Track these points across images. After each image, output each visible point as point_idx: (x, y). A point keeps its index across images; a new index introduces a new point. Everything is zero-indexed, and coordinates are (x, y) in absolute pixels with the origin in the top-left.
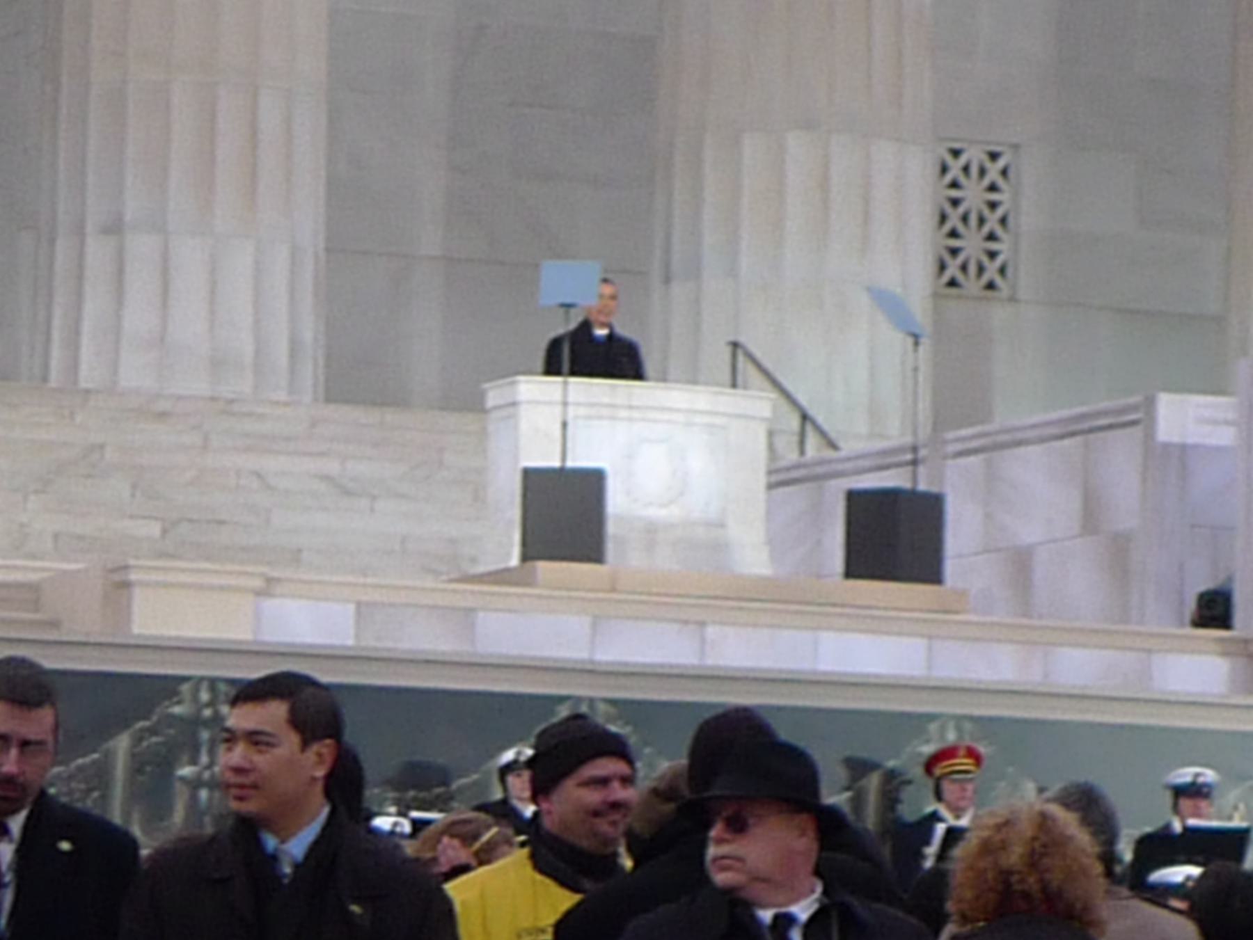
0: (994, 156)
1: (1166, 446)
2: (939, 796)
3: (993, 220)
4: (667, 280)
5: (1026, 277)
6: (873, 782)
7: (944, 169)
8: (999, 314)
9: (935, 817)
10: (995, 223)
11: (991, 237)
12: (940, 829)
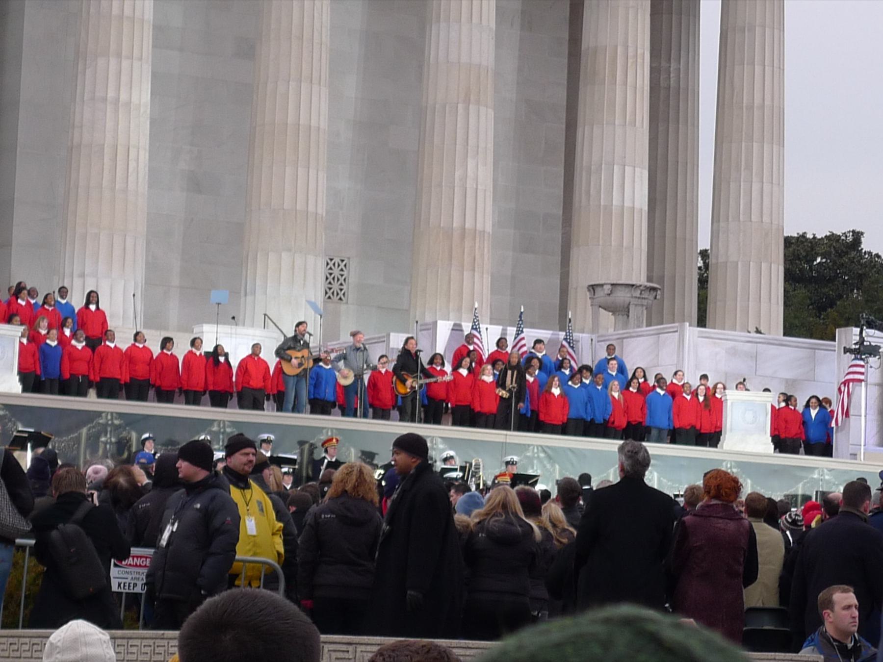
0: (342, 261)
1: (393, 349)
2: (326, 451)
3: (342, 280)
4: (246, 295)
5: (351, 296)
6: (307, 446)
7: (328, 264)
8: (343, 307)
9: (325, 458)
10: (342, 280)
11: (341, 284)
12: (326, 461)
